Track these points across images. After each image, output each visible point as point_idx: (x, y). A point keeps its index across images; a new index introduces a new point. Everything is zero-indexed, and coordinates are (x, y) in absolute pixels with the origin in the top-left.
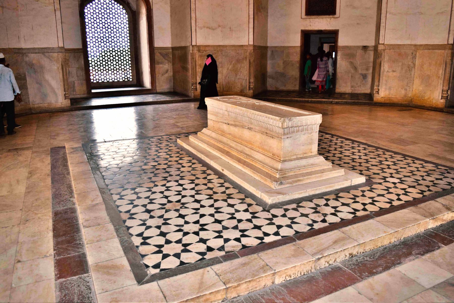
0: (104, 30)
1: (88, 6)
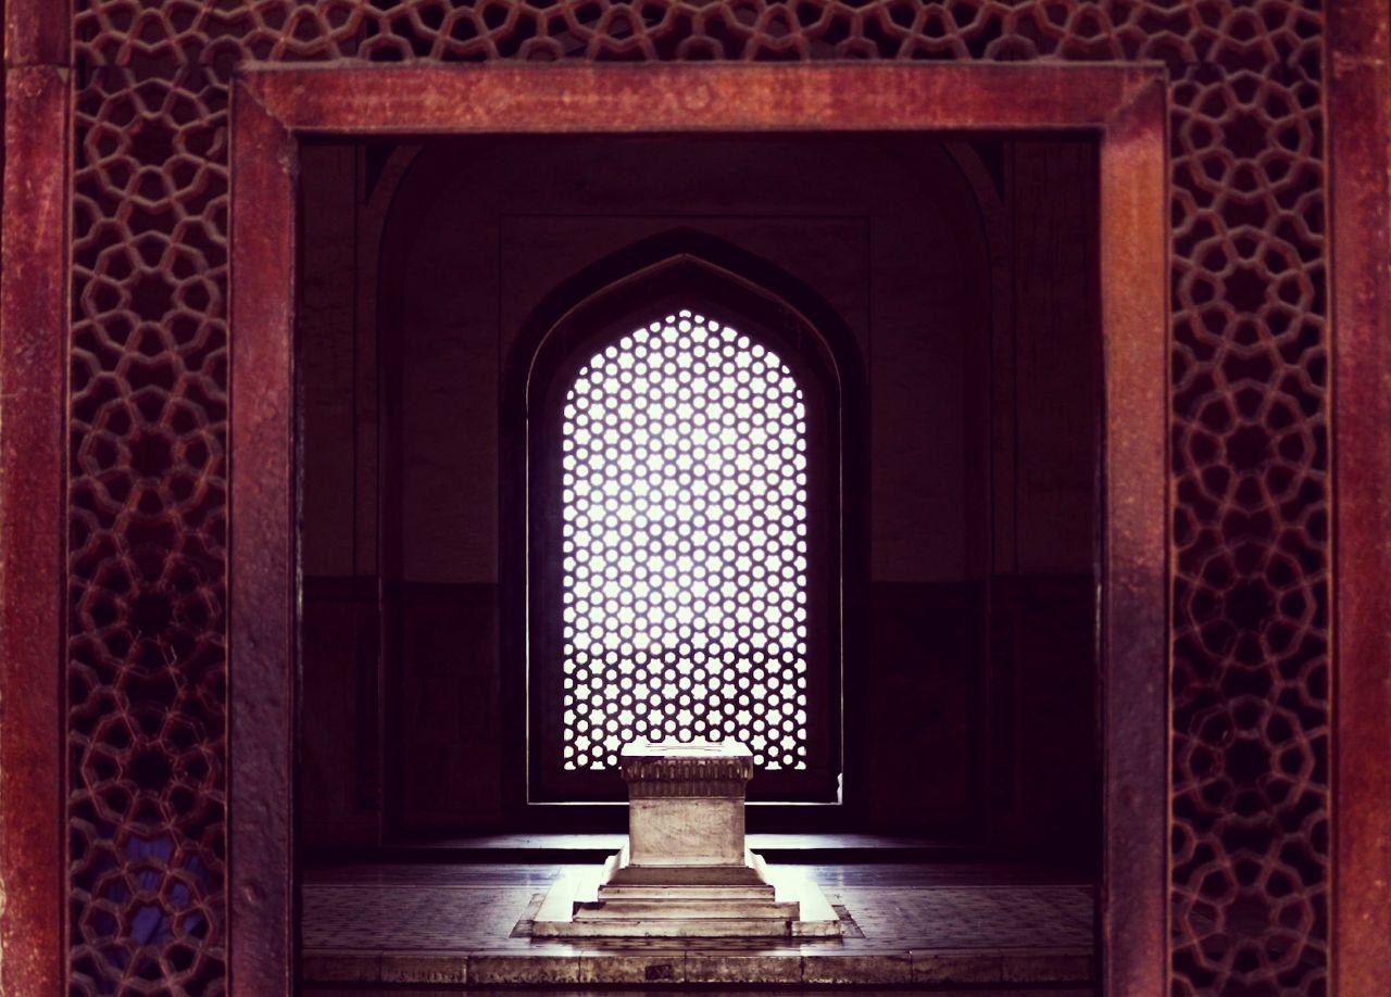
0: (670, 488)
1: (597, 361)
